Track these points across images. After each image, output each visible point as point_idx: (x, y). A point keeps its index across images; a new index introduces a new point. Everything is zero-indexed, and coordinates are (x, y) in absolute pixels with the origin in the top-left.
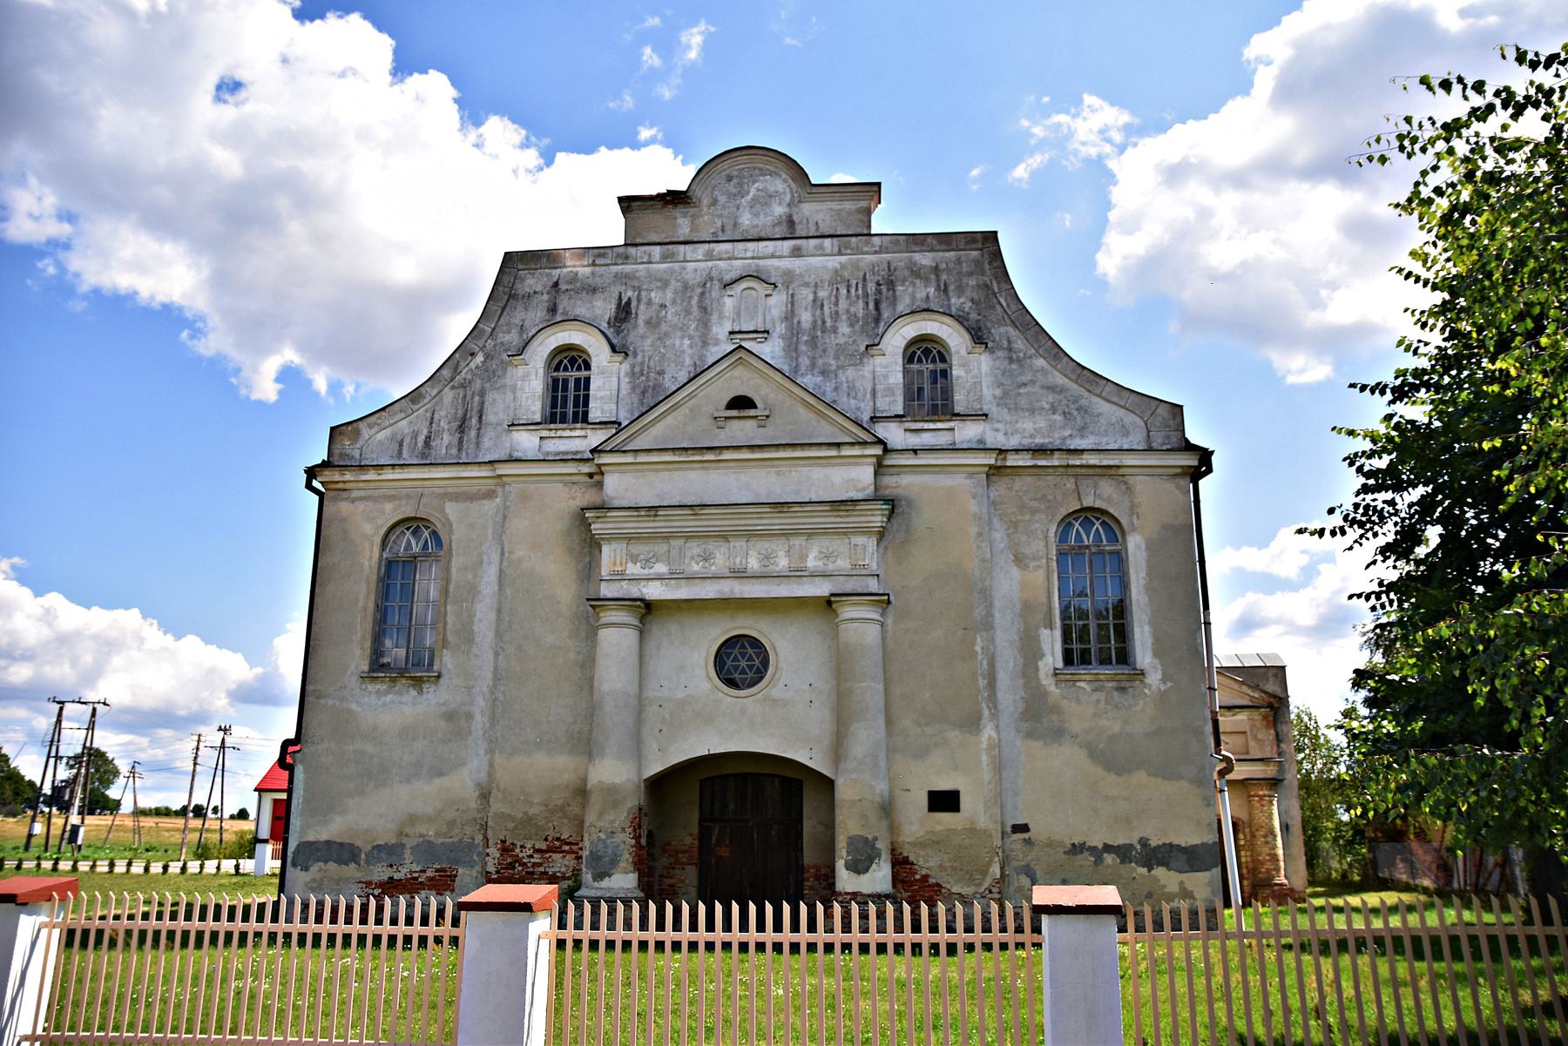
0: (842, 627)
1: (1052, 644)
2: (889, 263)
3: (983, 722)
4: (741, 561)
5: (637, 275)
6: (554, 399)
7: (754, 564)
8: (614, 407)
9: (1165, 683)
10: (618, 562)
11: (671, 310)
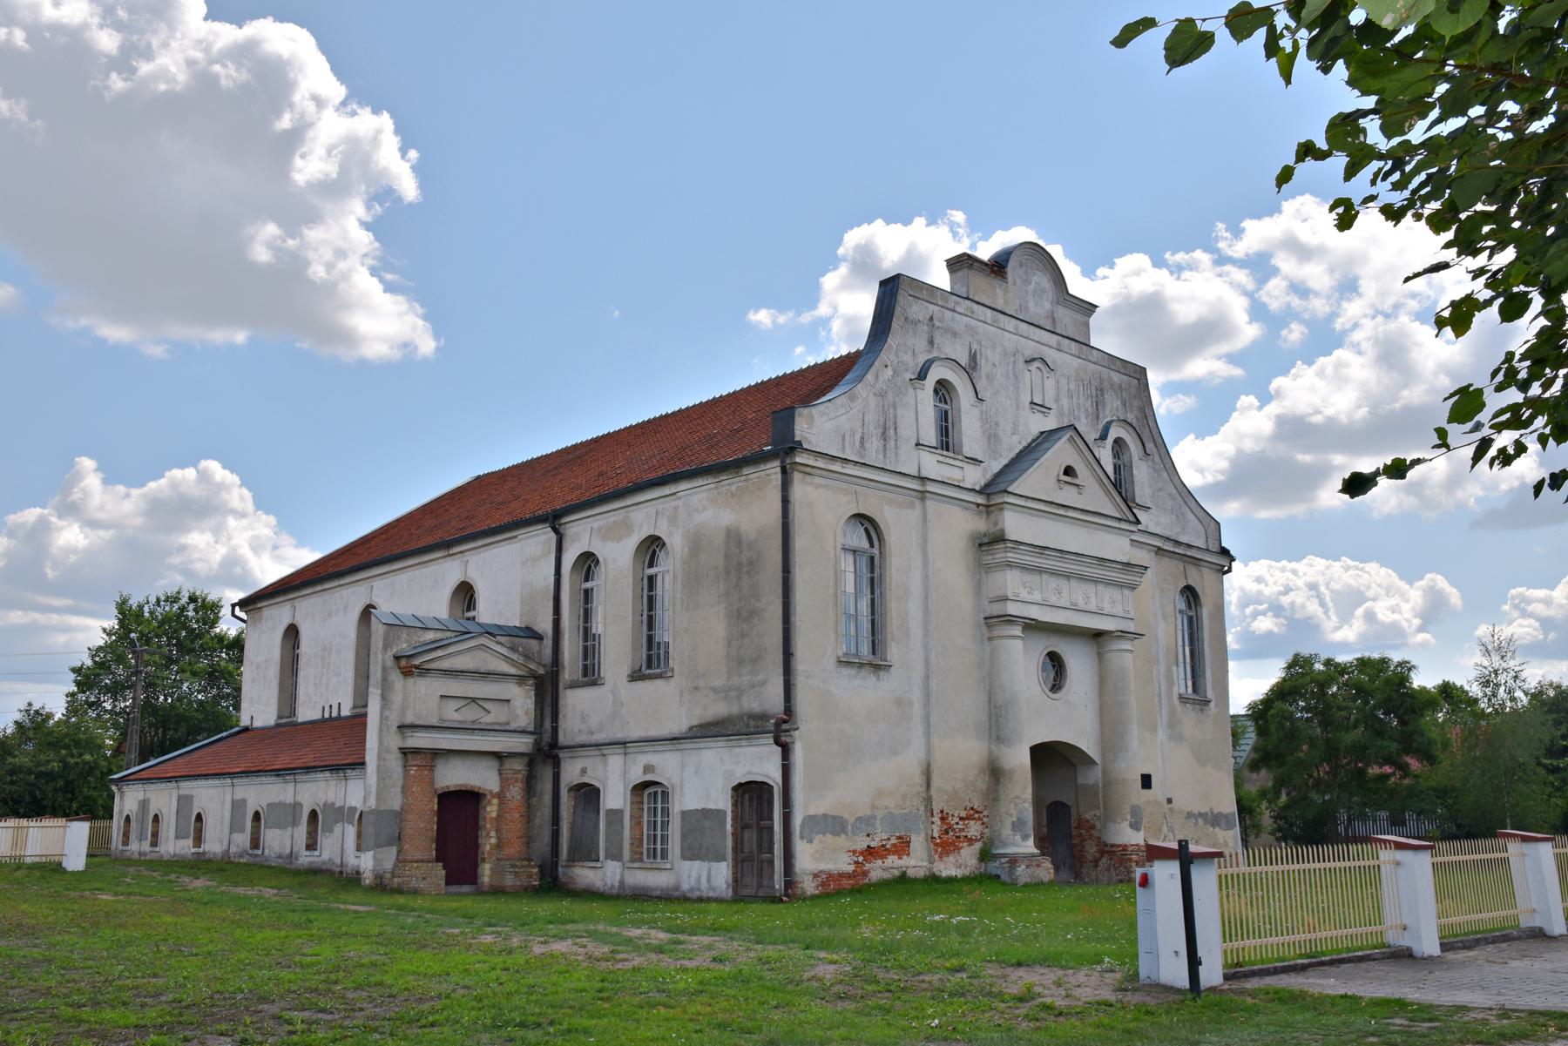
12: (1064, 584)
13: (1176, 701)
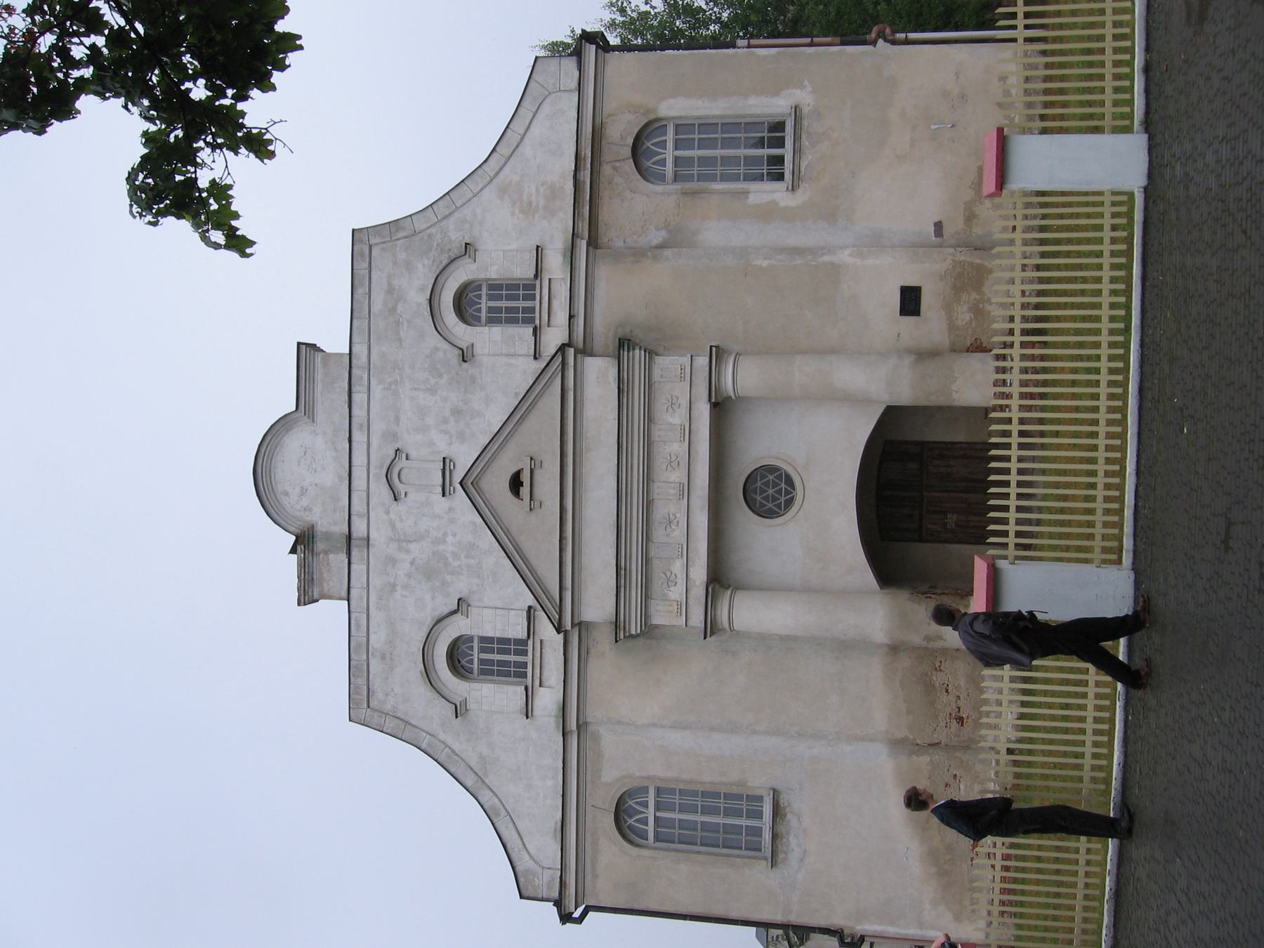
0: (741, 392)
1: (765, 193)
4: (674, 488)
6: (500, 674)
7: (678, 476)
8: (512, 613)
10: (671, 608)
12: (661, 510)
13: (802, 196)
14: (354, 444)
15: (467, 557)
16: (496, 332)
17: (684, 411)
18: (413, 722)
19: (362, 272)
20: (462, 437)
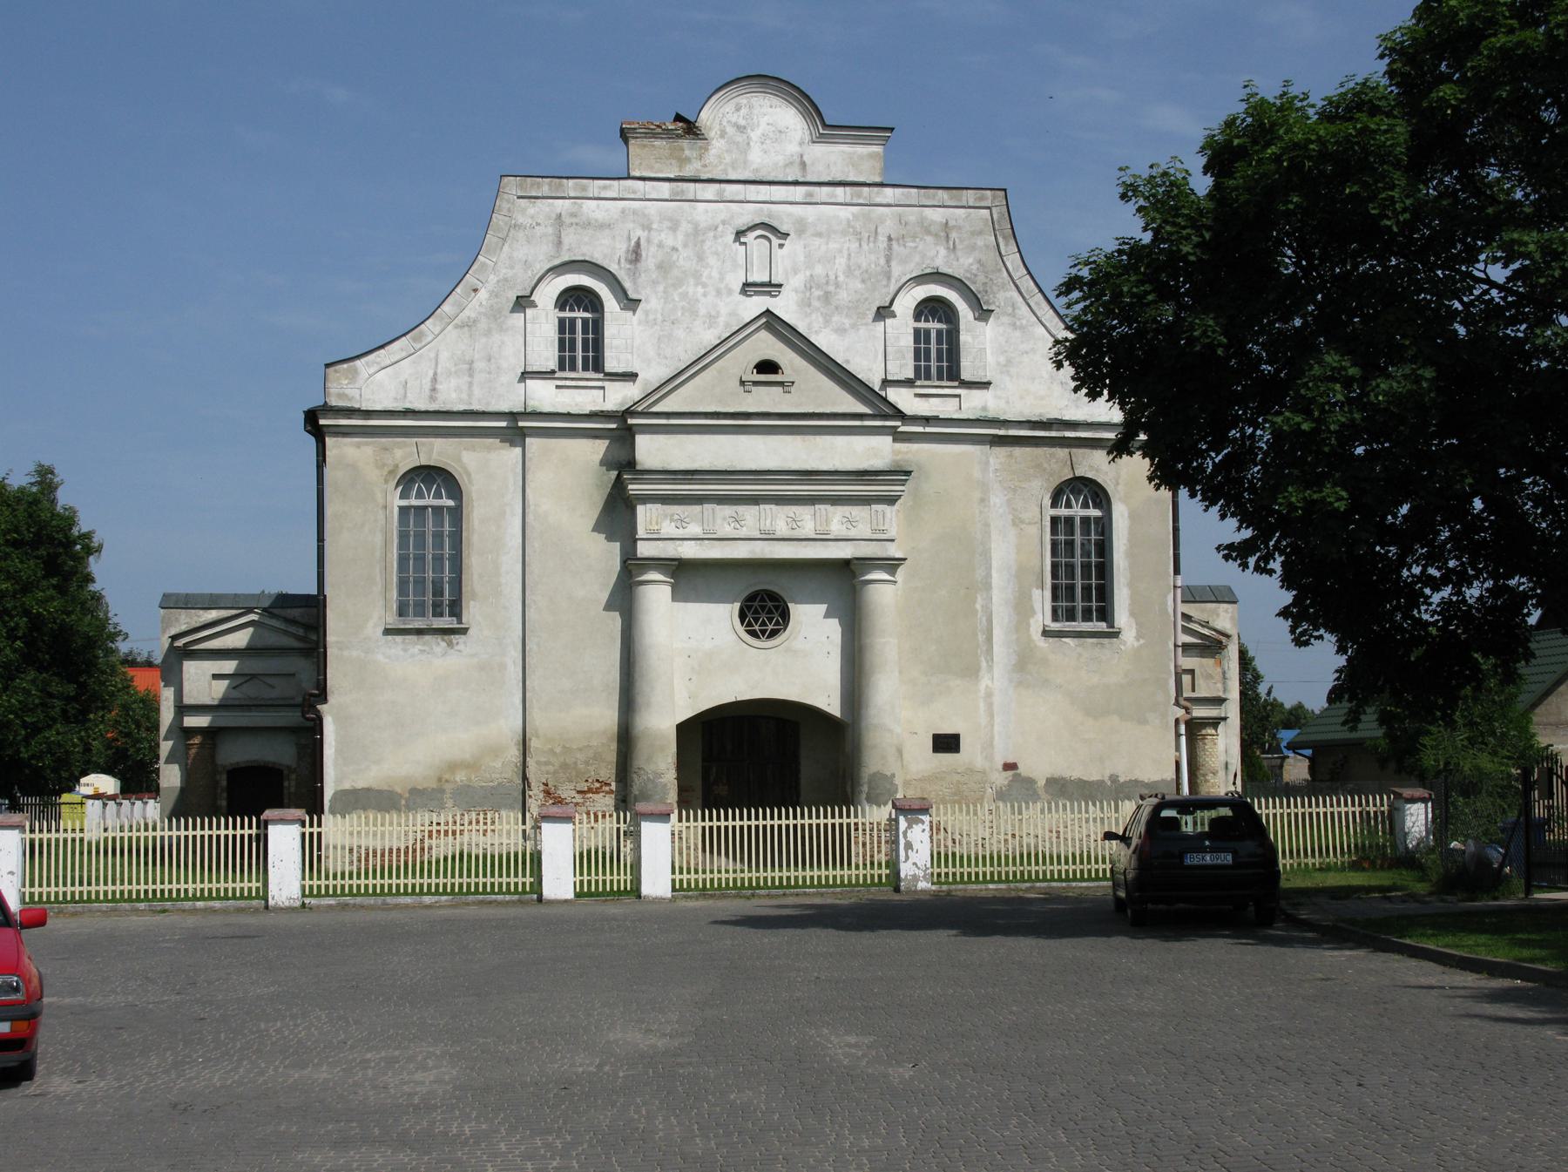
2: (900, 216)
3: (980, 674)
5: (646, 212)
6: (561, 342)
7: (782, 529)
9: (1138, 640)
10: (654, 523)
11: (684, 253)
12: (749, 513)
14: (791, 188)
15: (683, 308)
16: (908, 341)
17: (844, 533)
18: (506, 246)
19: (964, 198)
20: (805, 304)
